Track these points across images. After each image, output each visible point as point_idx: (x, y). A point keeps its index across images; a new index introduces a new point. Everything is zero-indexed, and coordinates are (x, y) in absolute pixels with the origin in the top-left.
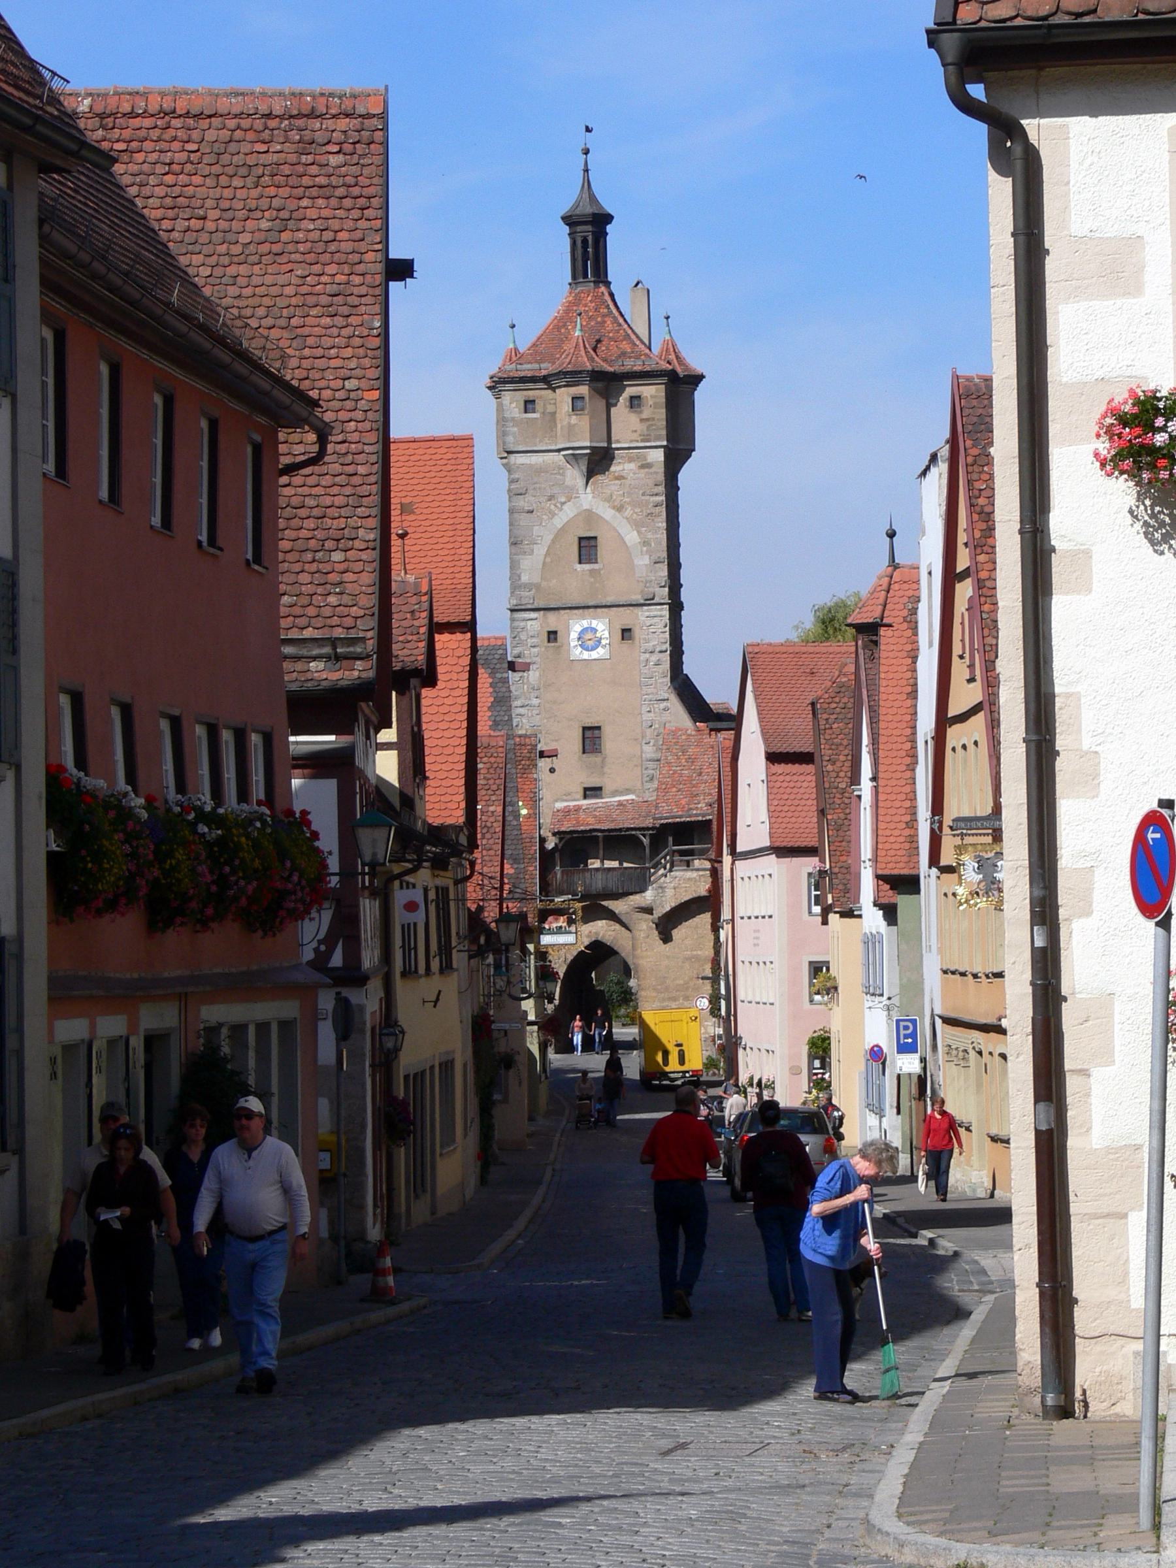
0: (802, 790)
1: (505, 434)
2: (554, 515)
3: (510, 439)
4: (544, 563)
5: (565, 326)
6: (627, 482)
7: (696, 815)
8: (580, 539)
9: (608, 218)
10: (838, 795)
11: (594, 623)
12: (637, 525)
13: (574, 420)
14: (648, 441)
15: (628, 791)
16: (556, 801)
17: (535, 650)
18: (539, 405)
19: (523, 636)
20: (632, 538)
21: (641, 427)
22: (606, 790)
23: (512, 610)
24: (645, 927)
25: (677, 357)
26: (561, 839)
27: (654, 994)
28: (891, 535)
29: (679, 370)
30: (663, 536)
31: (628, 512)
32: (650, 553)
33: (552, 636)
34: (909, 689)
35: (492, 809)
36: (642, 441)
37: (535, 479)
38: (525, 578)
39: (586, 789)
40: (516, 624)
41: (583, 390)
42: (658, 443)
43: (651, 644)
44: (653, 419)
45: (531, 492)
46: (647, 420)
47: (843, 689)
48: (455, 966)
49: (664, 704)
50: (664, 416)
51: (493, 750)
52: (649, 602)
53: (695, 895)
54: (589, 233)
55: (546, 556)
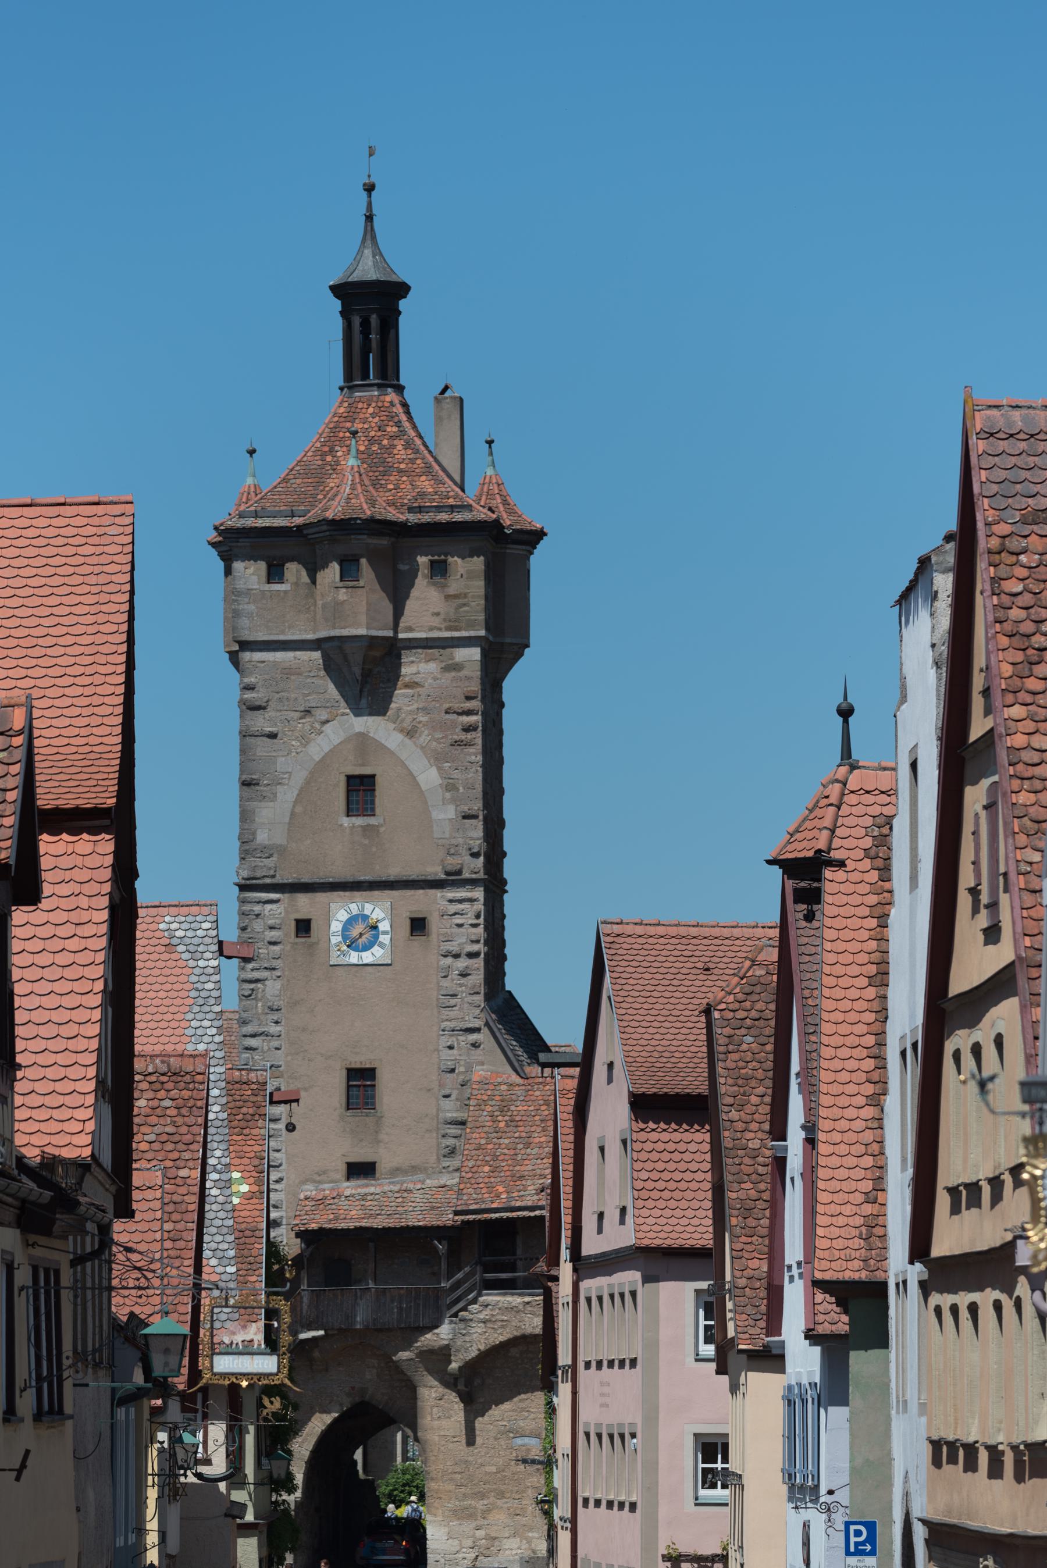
0: (687, 1157)
1: (236, 614)
2: (305, 740)
3: (244, 622)
4: (293, 814)
5: (332, 451)
7: (520, 1209)
8: (350, 778)
9: (402, 289)
10: (746, 1160)
11: (368, 908)
12: (437, 759)
13: (342, 595)
14: (456, 629)
15: (414, 1169)
16: (304, 1182)
19: (258, 926)
20: (429, 777)
22: (382, 1168)
23: (243, 888)
25: (505, 503)
27: (451, 1487)
28: (846, 713)
29: (506, 521)
30: (476, 776)
31: (424, 738)
32: (454, 800)
33: (303, 927)
34: (873, 969)
35: (183, 1173)
36: (449, 629)
40: (247, 908)
43: (454, 943)
44: (465, 595)
46: (456, 596)
47: (758, 989)
48: (68, 1409)
50: (482, 592)
51: (188, 1078)
53: (516, 1333)
54: (371, 311)
55: (296, 802)
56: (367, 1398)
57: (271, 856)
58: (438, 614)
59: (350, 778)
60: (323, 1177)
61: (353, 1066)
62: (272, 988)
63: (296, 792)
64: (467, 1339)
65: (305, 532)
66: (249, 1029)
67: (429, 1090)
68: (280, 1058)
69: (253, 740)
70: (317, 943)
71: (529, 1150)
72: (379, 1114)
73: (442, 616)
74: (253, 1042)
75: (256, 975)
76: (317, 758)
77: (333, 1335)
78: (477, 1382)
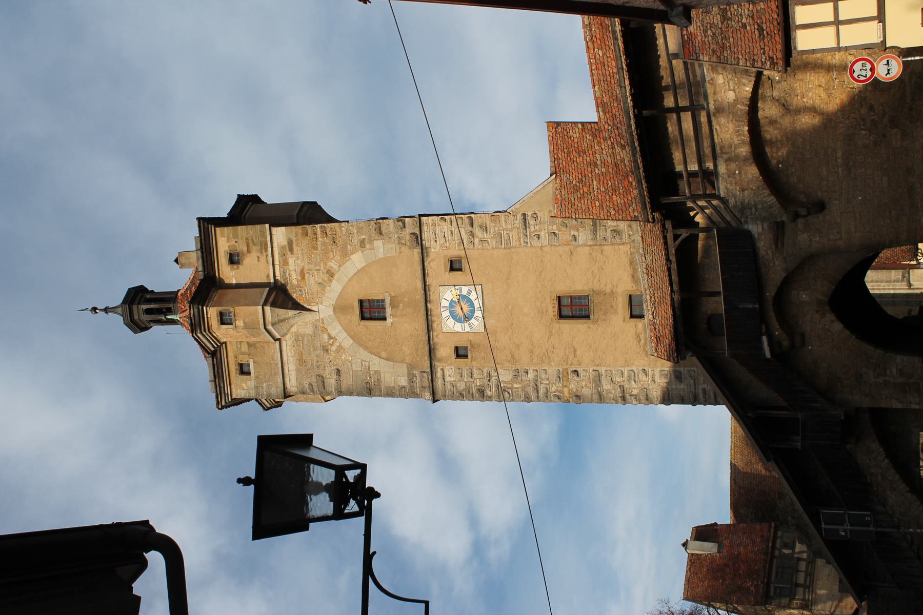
2: (340, 348)
6: (306, 267)
7: (636, 161)
8: (363, 318)
11: (445, 303)
12: (345, 254)
13: (240, 323)
14: (266, 244)
18: (243, 359)
19: (461, 386)
20: (357, 260)
21: (254, 254)
24: (805, 235)
31: (333, 265)
32: (371, 241)
33: (460, 353)
36: (266, 251)
37: (309, 366)
38: (403, 382)
39: (632, 316)
41: (212, 313)
42: (268, 233)
44: (247, 239)
45: (321, 372)
46: (248, 246)
49: (529, 218)
52: (418, 239)
55: (380, 357)
58: (258, 258)
59: (363, 318)
60: (642, 336)
61: (556, 313)
62: (505, 376)
63: (373, 357)
64: (760, 206)
66: (533, 395)
68: (552, 371)
71: (599, 163)
73: (259, 254)
74: (542, 391)
76: (351, 341)
77: (767, 328)
78: (802, 198)
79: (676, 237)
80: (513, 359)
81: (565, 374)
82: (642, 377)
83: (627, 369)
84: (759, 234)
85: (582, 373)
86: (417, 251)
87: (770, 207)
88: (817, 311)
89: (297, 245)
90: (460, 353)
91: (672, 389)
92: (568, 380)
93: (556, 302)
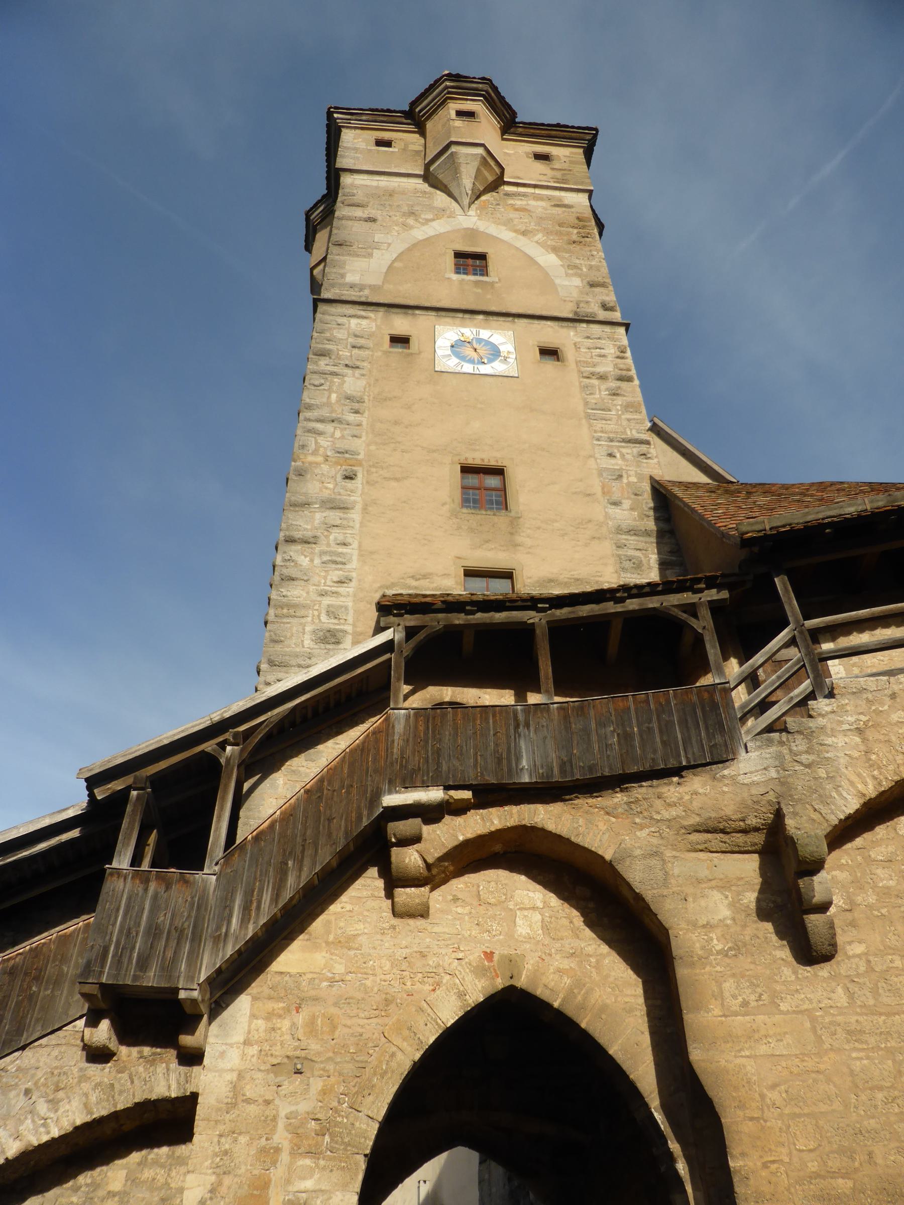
4: (390, 267)
11: (485, 334)
12: (555, 250)
17: (363, 353)
20: (549, 260)
24: (724, 912)
26: (410, 632)
49: (644, 448)
56: (522, 982)
57: (361, 290)
61: (470, 461)
65: (417, 110)
67: (589, 495)
68: (359, 445)
69: (350, 223)
70: (420, 353)
72: (513, 514)
74: (319, 426)
75: (335, 369)
79: (691, 609)
80: (382, 400)
81: (351, 462)
82: (335, 575)
83: (356, 553)
84: (733, 778)
85: (349, 484)
86: (571, 316)
87: (825, 800)
88: (489, 956)
89: (564, 212)
90: (400, 340)
91: (304, 625)
92: (337, 463)
93: (493, 463)
